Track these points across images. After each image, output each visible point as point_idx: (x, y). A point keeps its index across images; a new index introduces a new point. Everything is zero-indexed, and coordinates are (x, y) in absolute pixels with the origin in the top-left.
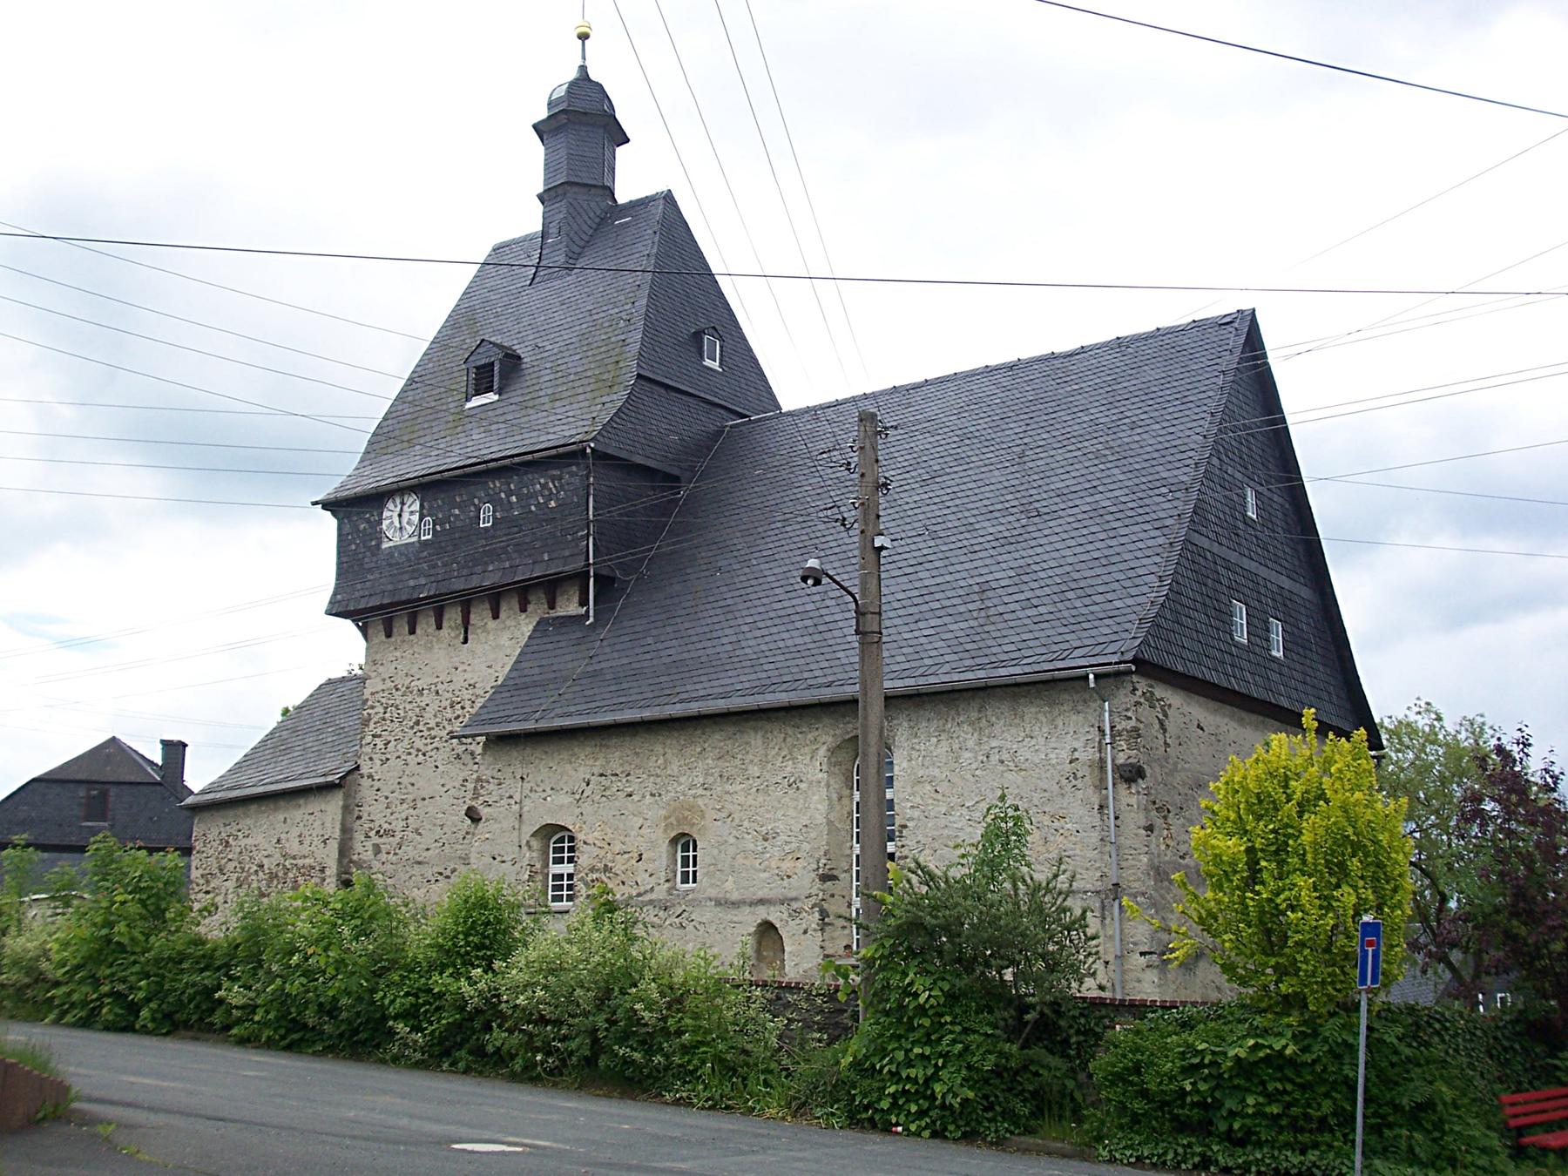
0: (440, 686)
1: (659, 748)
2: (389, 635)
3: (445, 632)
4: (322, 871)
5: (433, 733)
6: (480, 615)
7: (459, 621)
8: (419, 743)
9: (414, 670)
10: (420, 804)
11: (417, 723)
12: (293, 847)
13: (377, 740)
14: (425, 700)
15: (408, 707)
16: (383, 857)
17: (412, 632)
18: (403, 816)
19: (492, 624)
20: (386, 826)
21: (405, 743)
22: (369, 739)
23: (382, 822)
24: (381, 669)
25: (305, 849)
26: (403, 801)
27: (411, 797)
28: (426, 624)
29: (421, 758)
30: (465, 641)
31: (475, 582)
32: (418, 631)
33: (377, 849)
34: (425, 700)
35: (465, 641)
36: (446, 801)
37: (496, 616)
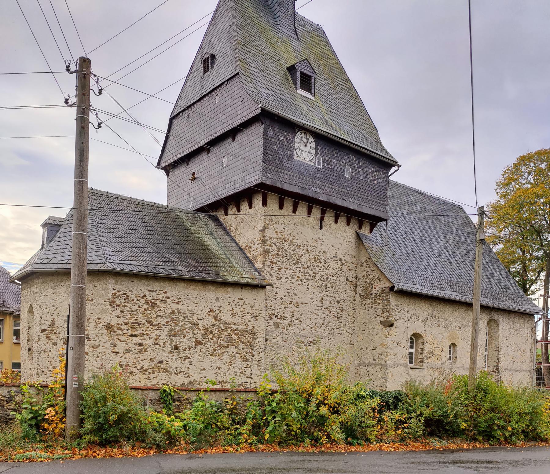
0: (309, 248)
1: (447, 310)
2: (294, 211)
3: (311, 219)
4: (254, 333)
5: (306, 270)
6: (329, 219)
7: (319, 217)
8: (298, 274)
9: (294, 234)
10: (300, 306)
11: (297, 263)
12: (228, 317)
13: (274, 266)
14: (301, 252)
15: (292, 252)
16: (280, 330)
17: (294, 211)
18: (291, 310)
19: (334, 225)
20: (281, 314)
21: (291, 272)
22: (269, 263)
23: (279, 311)
24: (275, 226)
25: (237, 319)
26: (291, 303)
27: (295, 301)
28: (302, 210)
29: (300, 282)
30: (321, 228)
31: (345, 204)
32: (297, 213)
33: (277, 326)
34: (301, 252)
35: (321, 228)
36: (313, 307)
37: (336, 222)
